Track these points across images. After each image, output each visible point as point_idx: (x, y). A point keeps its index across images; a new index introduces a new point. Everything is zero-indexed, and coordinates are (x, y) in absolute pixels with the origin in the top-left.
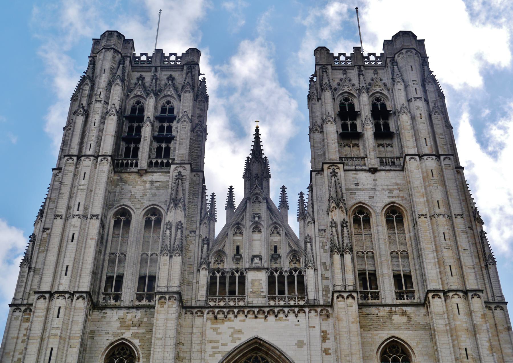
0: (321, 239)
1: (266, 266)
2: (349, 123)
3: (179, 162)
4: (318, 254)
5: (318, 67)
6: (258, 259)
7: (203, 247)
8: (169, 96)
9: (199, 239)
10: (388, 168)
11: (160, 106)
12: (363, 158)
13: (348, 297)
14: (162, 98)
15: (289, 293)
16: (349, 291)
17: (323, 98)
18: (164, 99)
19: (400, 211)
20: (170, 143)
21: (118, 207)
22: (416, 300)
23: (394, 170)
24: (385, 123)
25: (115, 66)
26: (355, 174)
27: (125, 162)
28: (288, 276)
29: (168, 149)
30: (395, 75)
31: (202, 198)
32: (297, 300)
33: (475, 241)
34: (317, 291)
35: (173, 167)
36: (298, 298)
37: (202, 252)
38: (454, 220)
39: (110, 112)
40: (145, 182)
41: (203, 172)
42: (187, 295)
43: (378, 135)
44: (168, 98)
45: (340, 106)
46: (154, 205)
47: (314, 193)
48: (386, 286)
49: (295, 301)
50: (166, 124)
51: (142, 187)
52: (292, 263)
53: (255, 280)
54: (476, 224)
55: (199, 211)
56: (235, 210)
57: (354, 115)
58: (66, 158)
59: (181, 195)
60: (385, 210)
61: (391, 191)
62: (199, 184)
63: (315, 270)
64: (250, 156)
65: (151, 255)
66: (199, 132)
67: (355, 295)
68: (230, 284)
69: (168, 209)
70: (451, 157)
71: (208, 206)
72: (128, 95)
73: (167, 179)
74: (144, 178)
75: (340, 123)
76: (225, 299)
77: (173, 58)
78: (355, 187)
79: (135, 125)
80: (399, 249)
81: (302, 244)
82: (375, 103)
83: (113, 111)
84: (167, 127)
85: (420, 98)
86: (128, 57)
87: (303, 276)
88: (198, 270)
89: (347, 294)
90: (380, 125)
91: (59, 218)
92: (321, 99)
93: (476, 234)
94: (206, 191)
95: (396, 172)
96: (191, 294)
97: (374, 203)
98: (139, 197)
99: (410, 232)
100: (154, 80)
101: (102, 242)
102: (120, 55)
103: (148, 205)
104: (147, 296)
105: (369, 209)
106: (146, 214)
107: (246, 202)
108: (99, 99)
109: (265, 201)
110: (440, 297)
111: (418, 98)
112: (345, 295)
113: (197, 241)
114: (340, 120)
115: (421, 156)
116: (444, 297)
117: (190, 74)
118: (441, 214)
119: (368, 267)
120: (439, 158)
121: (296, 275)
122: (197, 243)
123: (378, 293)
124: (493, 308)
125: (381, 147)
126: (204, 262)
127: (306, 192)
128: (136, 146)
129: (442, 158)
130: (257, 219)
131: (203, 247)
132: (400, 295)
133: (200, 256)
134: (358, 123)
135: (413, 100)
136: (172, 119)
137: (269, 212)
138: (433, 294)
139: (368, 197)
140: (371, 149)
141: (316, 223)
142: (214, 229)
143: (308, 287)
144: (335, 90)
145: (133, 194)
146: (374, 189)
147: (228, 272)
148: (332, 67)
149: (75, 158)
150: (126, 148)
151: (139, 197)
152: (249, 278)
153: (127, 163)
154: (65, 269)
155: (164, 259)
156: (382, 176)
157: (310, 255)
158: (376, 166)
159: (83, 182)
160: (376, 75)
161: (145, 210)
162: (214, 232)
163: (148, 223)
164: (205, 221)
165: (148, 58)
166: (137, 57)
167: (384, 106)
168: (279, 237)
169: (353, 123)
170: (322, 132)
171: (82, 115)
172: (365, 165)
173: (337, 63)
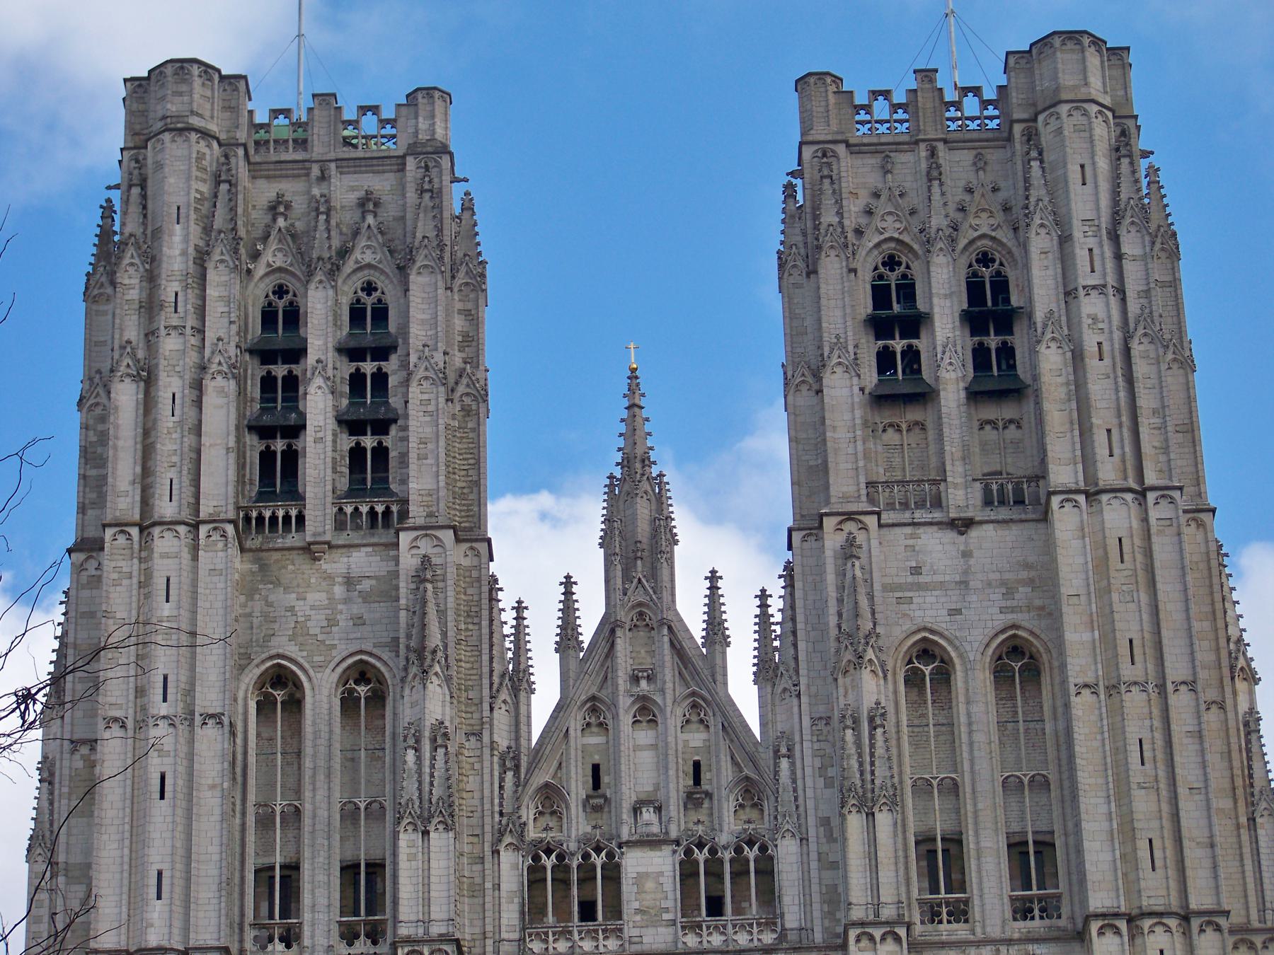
0: (816, 746)
1: (674, 834)
2: (898, 349)
3: (420, 521)
4: (810, 793)
5: (808, 152)
6: (652, 810)
7: (502, 780)
8: (369, 266)
9: (492, 755)
10: (1003, 513)
11: (346, 301)
12: (935, 482)
13: (883, 939)
14: (349, 275)
15: (738, 911)
16: (887, 923)
17: (821, 271)
18: (354, 278)
19: (1034, 650)
20: (386, 432)
21: (263, 662)
22: (1062, 923)
23: (1022, 521)
24: (1005, 343)
25: (205, 188)
26: (913, 536)
27: (267, 514)
28: (732, 861)
29: (381, 453)
30: (1033, 199)
31: (491, 621)
32: (755, 930)
33: (1229, 744)
34: (807, 905)
35: (405, 538)
36: (759, 924)
37: (501, 796)
38: (1173, 699)
39: (214, 367)
40: (329, 578)
41: (489, 541)
42: (472, 925)
43: (975, 395)
44: (366, 272)
45: (873, 287)
46: (361, 652)
47: (798, 594)
48: (986, 885)
49: (751, 933)
50: (369, 367)
51: (324, 595)
52: (744, 815)
53: (647, 874)
54: (1235, 693)
55: (486, 670)
56: (582, 654)
57: (914, 324)
58: (109, 532)
59: (434, 639)
60: (990, 651)
61: (1009, 593)
62: (479, 580)
63: (801, 840)
64: (618, 472)
65: (366, 808)
66: (467, 400)
67: (902, 932)
68: (581, 881)
69: (403, 680)
70: (1176, 494)
71: (508, 645)
72: (249, 271)
73: (391, 566)
74: (324, 565)
75: (869, 349)
76: (570, 933)
77: (369, 124)
78: (910, 579)
79: (280, 371)
80: (1026, 774)
81: (766, 757)
82: (975, 274)
83: (220, 364)
84: (373, 375)
85: (1101, 288)
86: (238, 145)
87: (771, 858)
88: (496, 852)
89: (882, 930)
90: (989, 350)
91: (115, 728)
92: (815, 272)
93: (1232, 723)
94: (500, 595)
95: (1026, 524)
96: (479, 923)
97: (960, 629)
98: (317, 631)
99: (1055, 719)
100: (323, 217)
101: (234, 779)
102: (215, 144)
103: (345, 654)
104: (368, 928)
105: (949, 649)
106: (344, 680)
107: (613, 631)
108: (175, 321)
109: (665, 631)
110: (1118, 932)
111: (1094, 287)
112: (877, 933)
113: (487, 764)
114: (872, 338)
115: (1093, 494)
116: (1129, 929)
117: (427, 196)
118: (1135, 683)
119: (940, 827)
120: (1145, 496)
121: (751, 854)
122: (487, 771)
123: (967, 902)
124: (1259, 945)
125: (988, 427)
126: (509, 827)
127: (776, 589)
128: (290, 446)
129: (1151, 496)
130: (643, 683)
131: (502, 780)
132: (1023, 911)
133: (497, 809)
134: (921, 344)
135: (1081, 292)
136: (382, 353)
137: (676, 659)
138: (1100, 923)
139: (945, 612)
140: (958, 455)
141: (804, 699)
142: (529, 717)
143: (783, 892)
144: (859, 232)
145: (300, 619)
146: (964, 584)
147: (573, 854)
148: (848, 145)
149: (134, 532)
150: (262, 453)
151: (317, 631)
152: (629, 869)
153: (274, 518)
154: (154, 881)
155: (407, 840)
156: (983, 536)
157: (787, 796)
158: (969, 514)
159: (166, 610)
160: (981, 173)
161: (340, 670)
162: (529, 725)
163: (349, 703)
164: (504, 695)
165: (298, 125)
166: (262, 126)
167: (1001, 286)
168: (703, 736)
169: (910, 346)
170: (819, 392)
171: (136, 378)
172: (938, 503)
173: (864, 129)
